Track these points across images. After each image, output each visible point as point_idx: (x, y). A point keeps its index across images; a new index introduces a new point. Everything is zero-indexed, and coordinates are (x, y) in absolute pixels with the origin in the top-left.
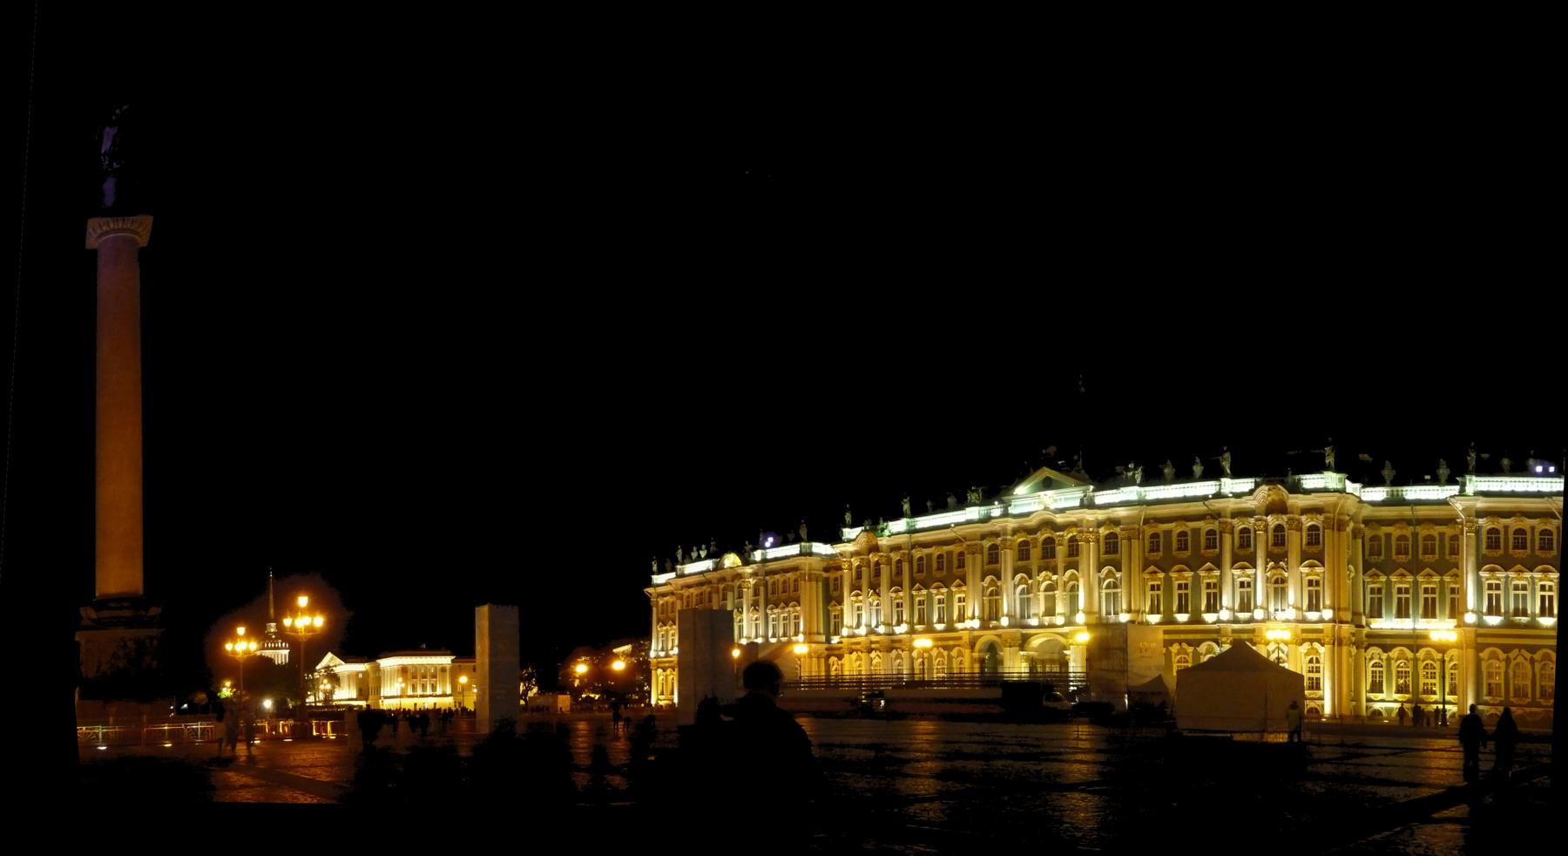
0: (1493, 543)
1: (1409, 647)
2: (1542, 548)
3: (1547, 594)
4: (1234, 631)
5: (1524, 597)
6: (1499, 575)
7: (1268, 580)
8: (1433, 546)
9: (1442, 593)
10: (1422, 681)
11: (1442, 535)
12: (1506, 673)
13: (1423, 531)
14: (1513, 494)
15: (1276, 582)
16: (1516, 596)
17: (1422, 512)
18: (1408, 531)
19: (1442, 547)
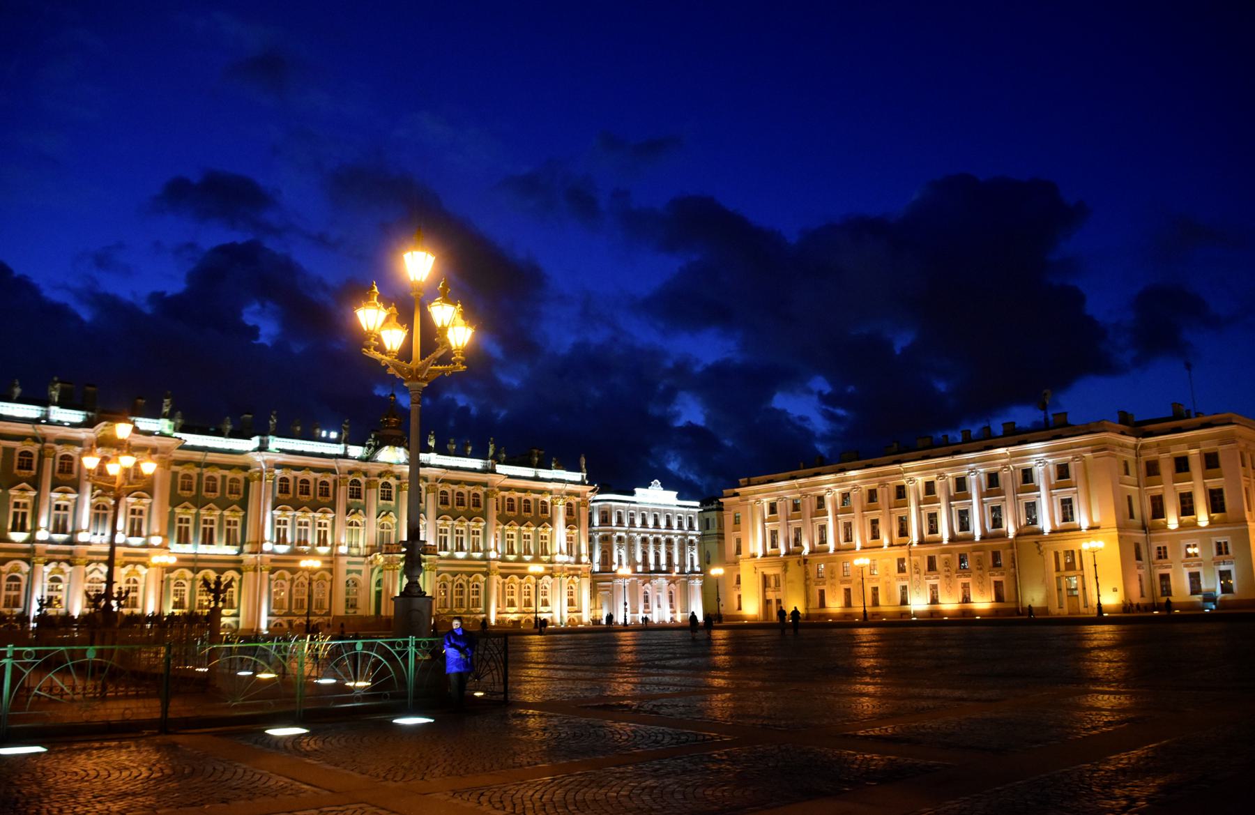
0: (284, 489)
1: (192, 569)
2: (321, 495)
3: (322, 529)
4: (49, 552)
5: (306, 531)
6: (288, 513)
7: (91, 505)
8: (215, 485)
9: (221, 525)
10: (198, 598)
11: (224, 477)
12: (290, 591)
13: (207, 472)
14: (302, 453)
15: (98, 508)
16: (300, 530)
17: (212, 457)
18: (194, 471)
19: (199, 484)
